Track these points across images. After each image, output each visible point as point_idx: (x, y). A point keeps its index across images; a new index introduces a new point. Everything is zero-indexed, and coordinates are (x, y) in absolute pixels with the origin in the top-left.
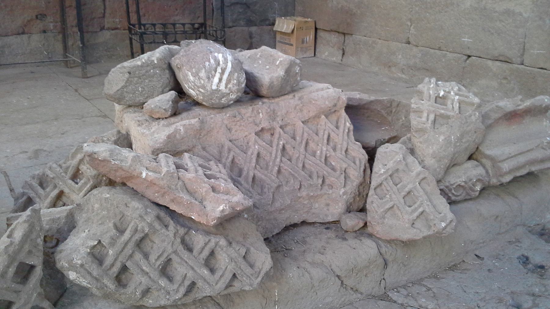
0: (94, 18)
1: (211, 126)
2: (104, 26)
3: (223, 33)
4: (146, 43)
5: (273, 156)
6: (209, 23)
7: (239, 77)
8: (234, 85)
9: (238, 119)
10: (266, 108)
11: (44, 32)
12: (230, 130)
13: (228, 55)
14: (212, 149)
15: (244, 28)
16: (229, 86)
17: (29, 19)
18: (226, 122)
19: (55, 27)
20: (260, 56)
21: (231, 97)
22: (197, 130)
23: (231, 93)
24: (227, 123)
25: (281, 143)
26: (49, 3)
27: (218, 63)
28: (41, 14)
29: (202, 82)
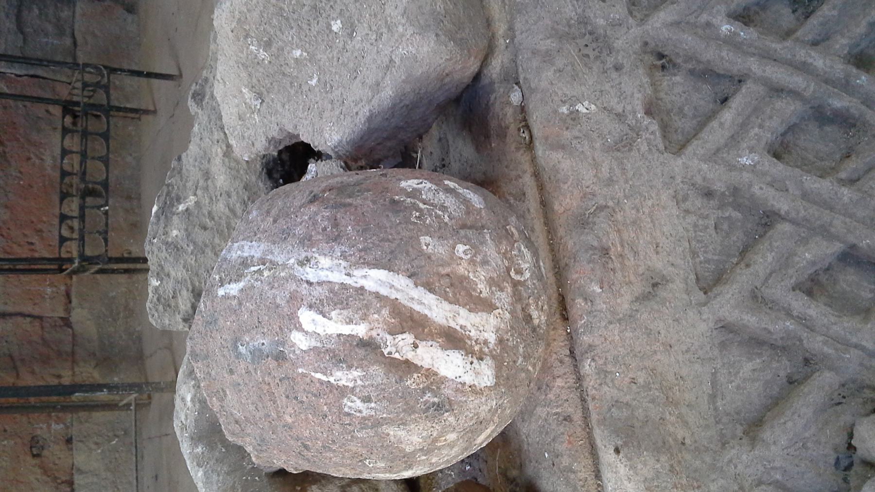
0: (43, 339)
1: (641, 381)
2: (62, 318)
3: (88, 69)
4: (106, 251)
5: (798, 81)
6: (64, 93)
7: (442, 226)
8: (479, 259)
9: (613, 236)
10: (549, 73)
11: (69, 441)
12: (657, 280)
13: (311, 274)
14: (738, 381)
15: (78, 10)
16: (483, 288)
17: (39, 471)
18: (624, 304)
19: (59, 421)
20: (268, 45)
21: (527, 275)
22: (672, 469)
23: (512, 274)
24: (628, 297)
25: (726, 28)
26: (5, 431)
27: (361, 352)
28: (31, 447)
29: (452, 437)
